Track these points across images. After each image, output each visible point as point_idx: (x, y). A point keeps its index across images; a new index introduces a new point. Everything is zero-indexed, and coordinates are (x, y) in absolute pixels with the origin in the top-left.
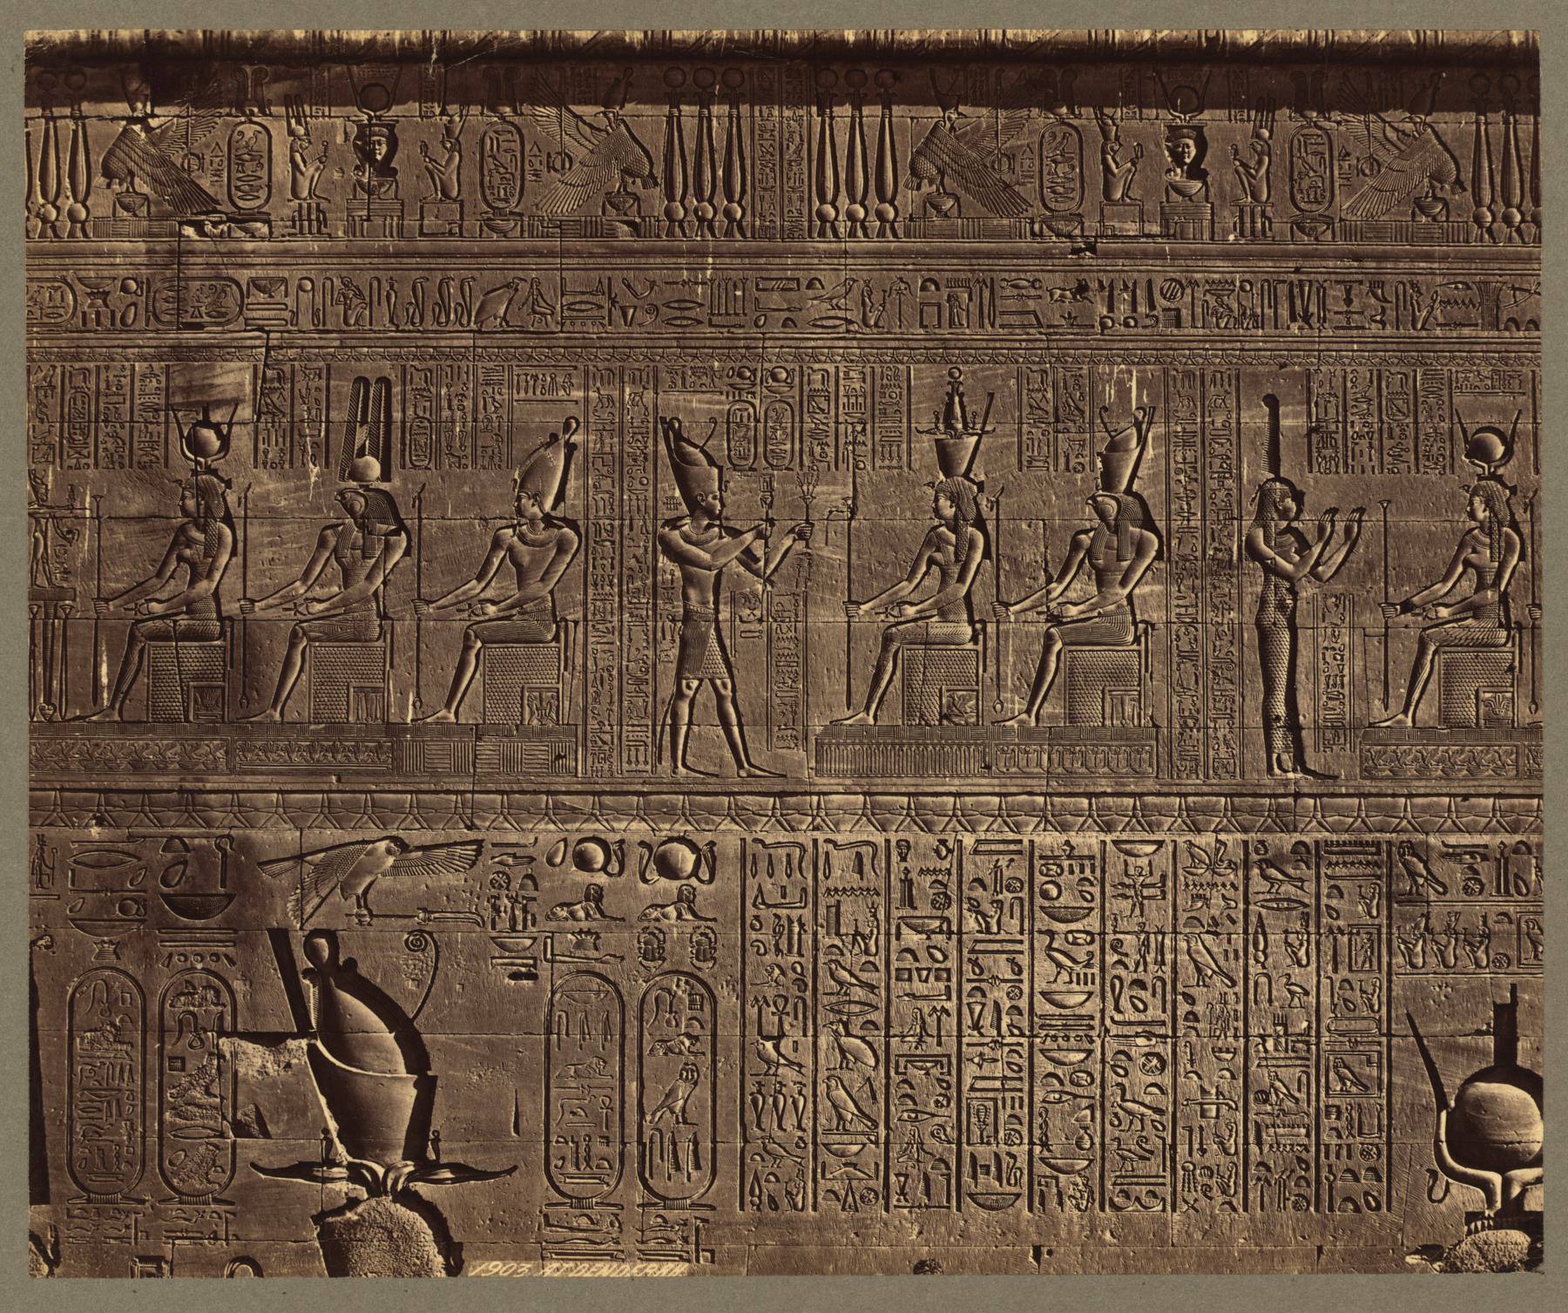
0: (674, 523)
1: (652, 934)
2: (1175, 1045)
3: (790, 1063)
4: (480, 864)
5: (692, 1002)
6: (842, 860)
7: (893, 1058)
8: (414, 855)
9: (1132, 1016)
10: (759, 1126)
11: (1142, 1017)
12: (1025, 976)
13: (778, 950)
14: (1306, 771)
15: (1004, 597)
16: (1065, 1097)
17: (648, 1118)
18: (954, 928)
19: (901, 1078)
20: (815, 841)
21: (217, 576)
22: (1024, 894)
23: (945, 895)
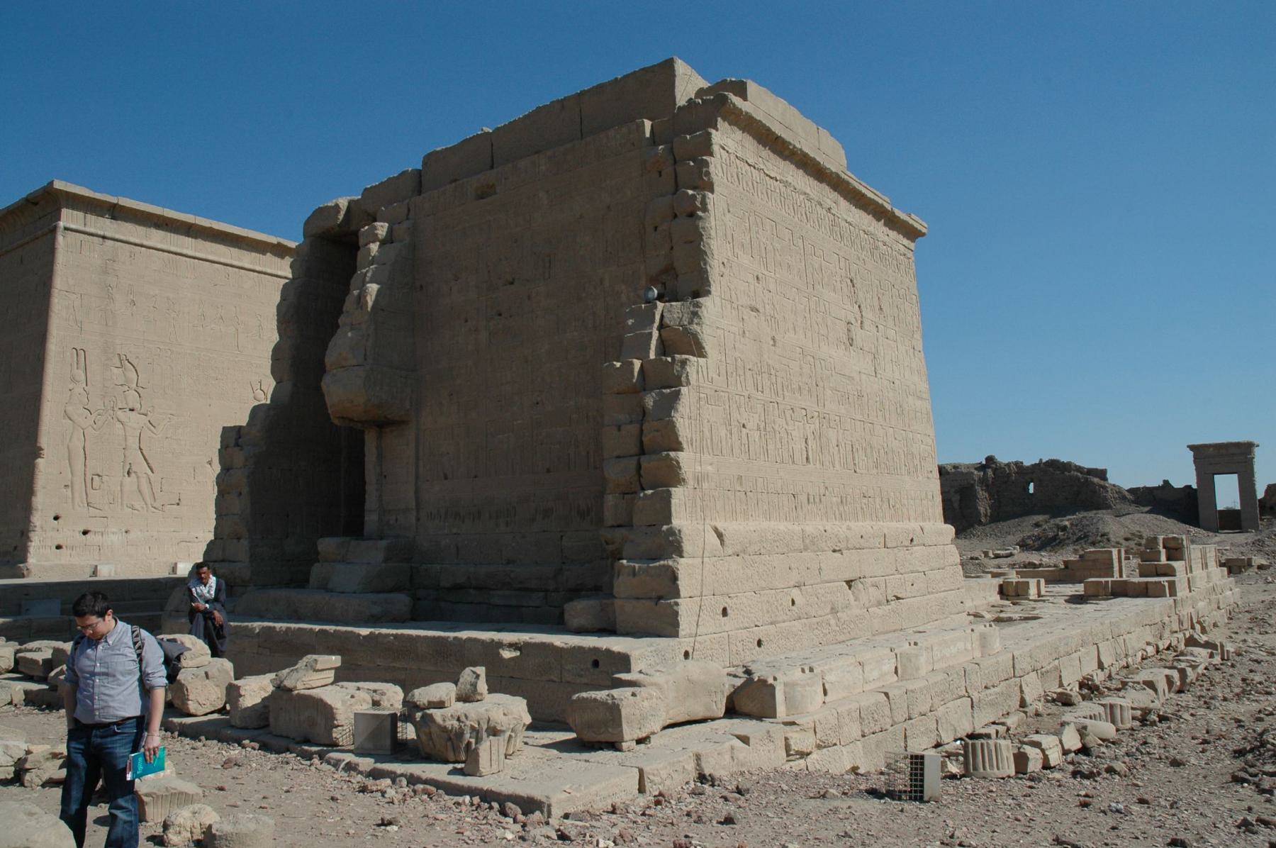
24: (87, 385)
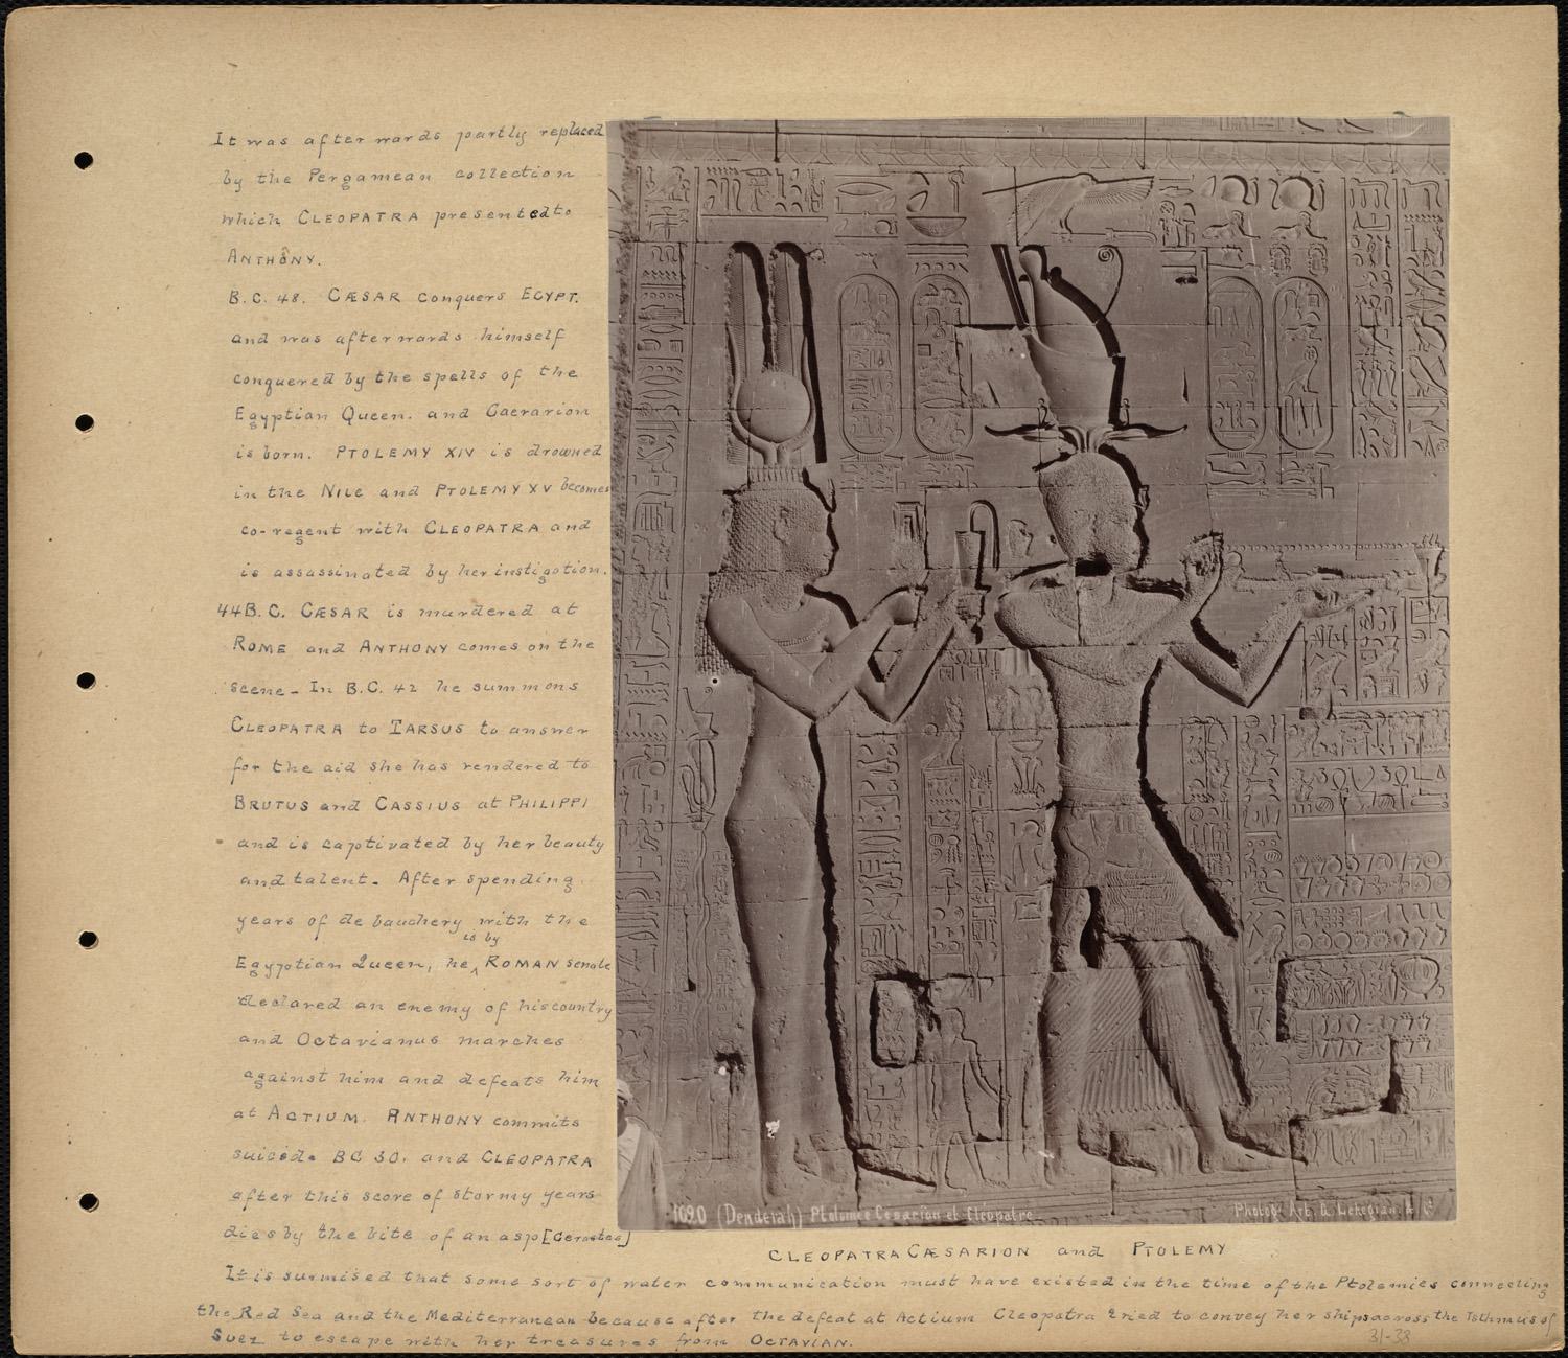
5: (1311, 301)
17: (1282, 388)
24: (821, 457)
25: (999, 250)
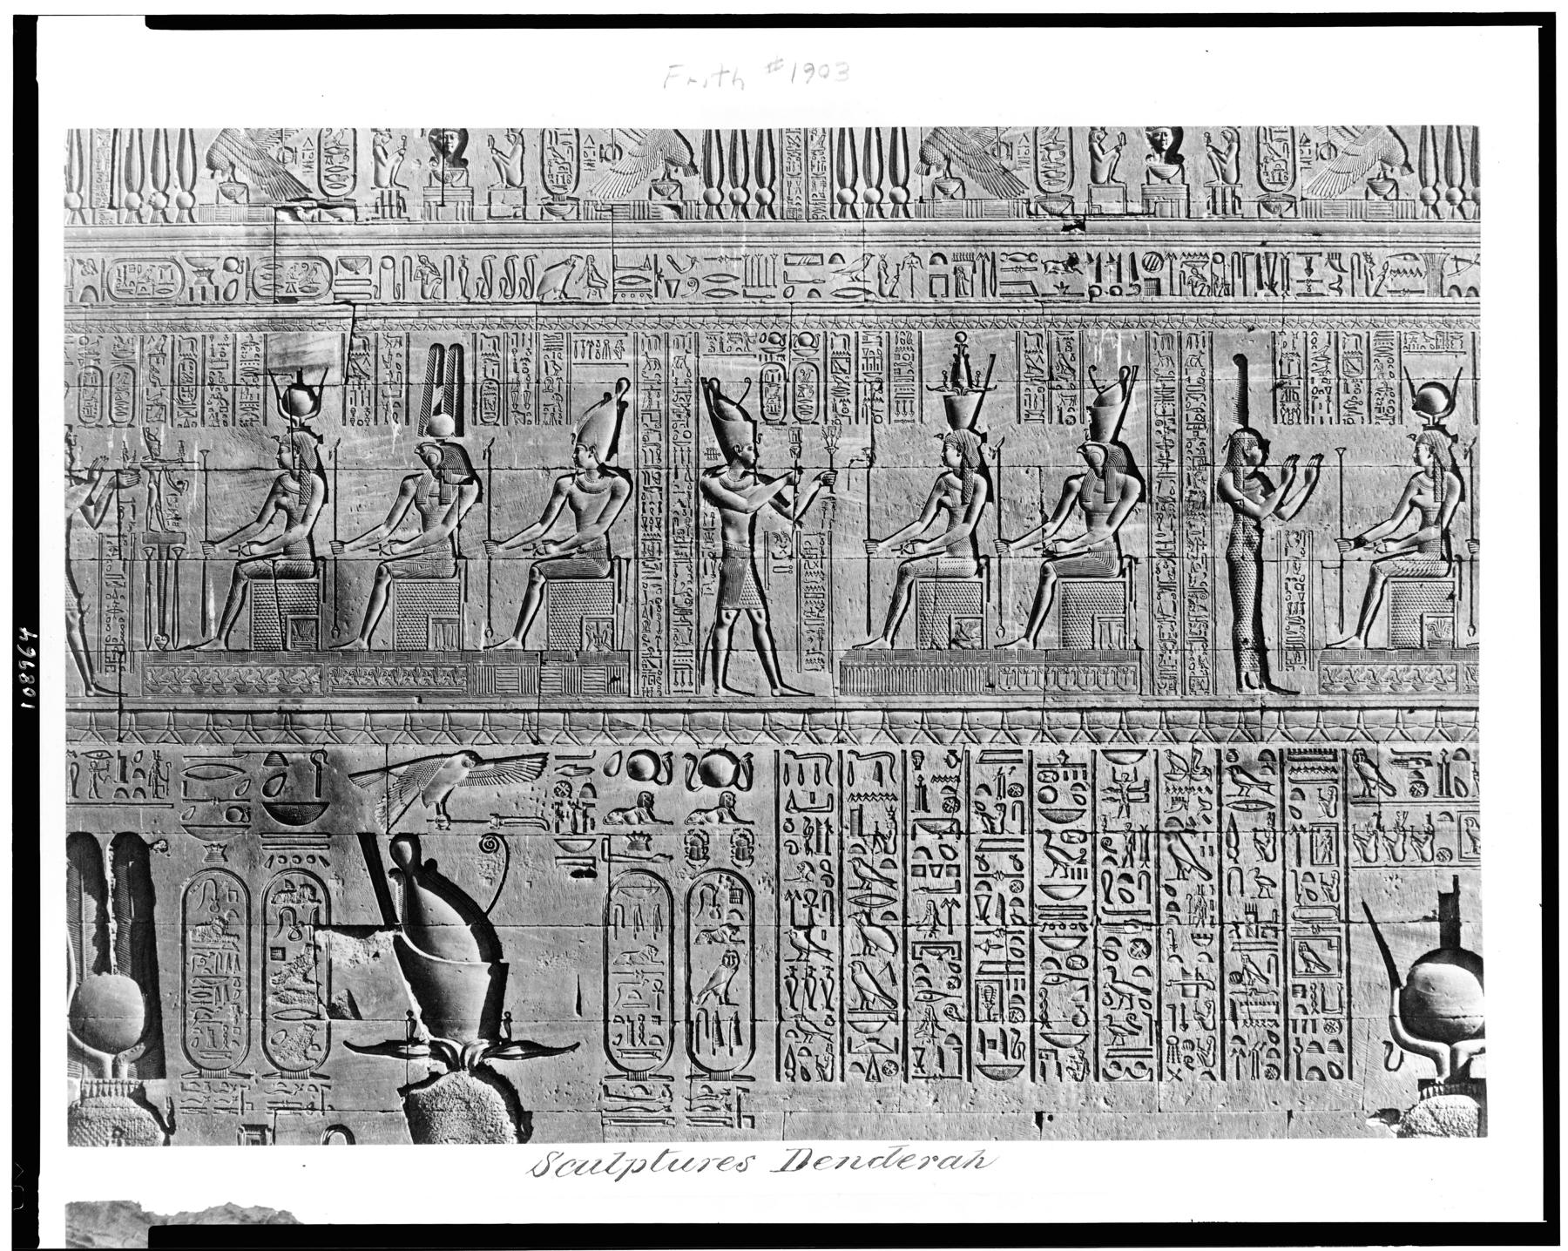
0: (713, 472)
1: (698, 836)
2: (1159, 932)
3: (820, 950)
4: (544, 774)
5: (732, 896)
6: (864, 769)
7: (910, 945)
8: (487, 767)
9: (1119, 905)
10: (792, 1005)
11: (1129, 907)
12: (1026, 871)
13: (808, 849)
14: (1272, 688)
15: (1005, 535)
16: (1062, 979)
17: (695, 999)
18: (963, 829)
19: (918, 962)
20: (840, 752)
21: (311, 520)
22: (1025, 798)
23: (955, 799)
25: (369, 841)
